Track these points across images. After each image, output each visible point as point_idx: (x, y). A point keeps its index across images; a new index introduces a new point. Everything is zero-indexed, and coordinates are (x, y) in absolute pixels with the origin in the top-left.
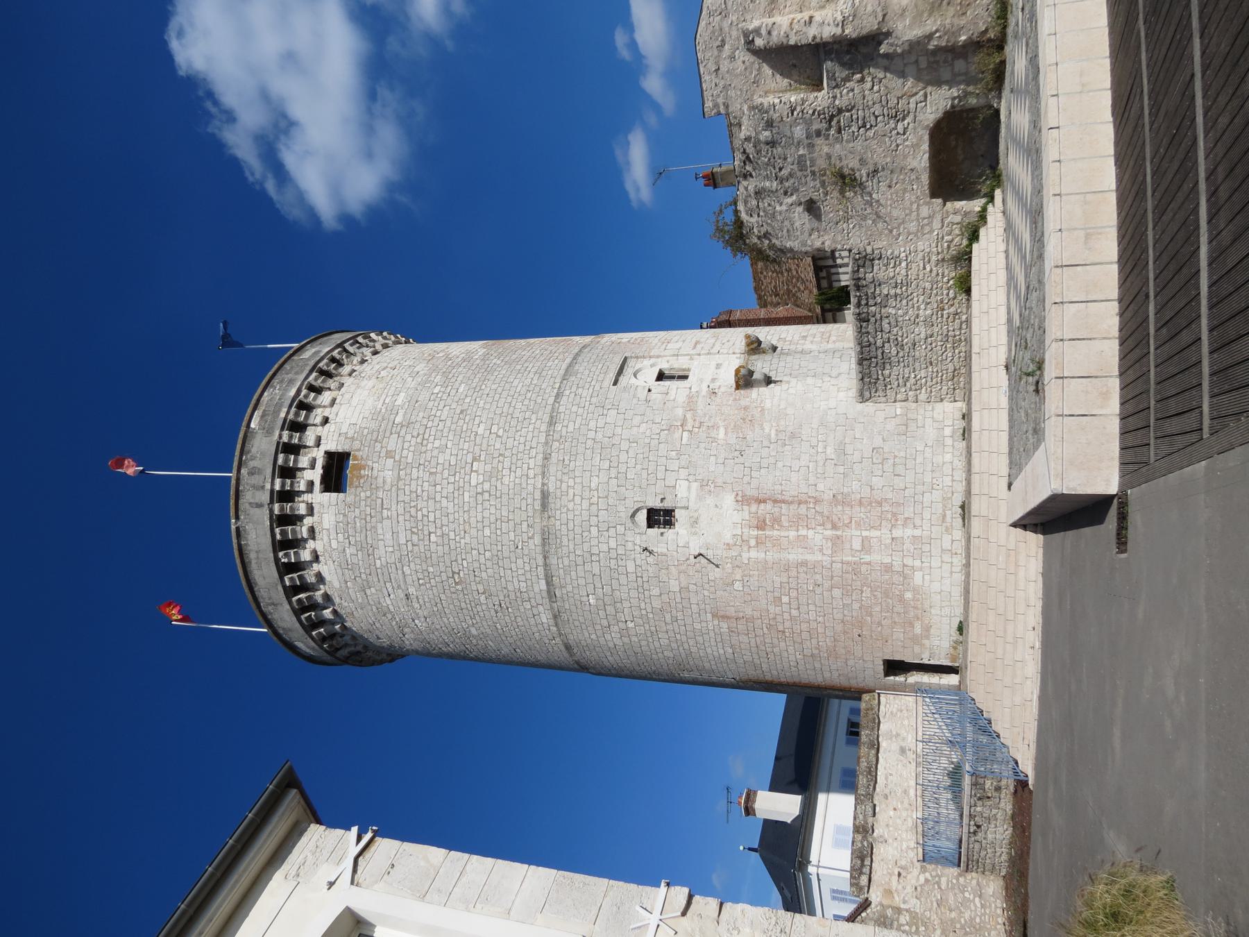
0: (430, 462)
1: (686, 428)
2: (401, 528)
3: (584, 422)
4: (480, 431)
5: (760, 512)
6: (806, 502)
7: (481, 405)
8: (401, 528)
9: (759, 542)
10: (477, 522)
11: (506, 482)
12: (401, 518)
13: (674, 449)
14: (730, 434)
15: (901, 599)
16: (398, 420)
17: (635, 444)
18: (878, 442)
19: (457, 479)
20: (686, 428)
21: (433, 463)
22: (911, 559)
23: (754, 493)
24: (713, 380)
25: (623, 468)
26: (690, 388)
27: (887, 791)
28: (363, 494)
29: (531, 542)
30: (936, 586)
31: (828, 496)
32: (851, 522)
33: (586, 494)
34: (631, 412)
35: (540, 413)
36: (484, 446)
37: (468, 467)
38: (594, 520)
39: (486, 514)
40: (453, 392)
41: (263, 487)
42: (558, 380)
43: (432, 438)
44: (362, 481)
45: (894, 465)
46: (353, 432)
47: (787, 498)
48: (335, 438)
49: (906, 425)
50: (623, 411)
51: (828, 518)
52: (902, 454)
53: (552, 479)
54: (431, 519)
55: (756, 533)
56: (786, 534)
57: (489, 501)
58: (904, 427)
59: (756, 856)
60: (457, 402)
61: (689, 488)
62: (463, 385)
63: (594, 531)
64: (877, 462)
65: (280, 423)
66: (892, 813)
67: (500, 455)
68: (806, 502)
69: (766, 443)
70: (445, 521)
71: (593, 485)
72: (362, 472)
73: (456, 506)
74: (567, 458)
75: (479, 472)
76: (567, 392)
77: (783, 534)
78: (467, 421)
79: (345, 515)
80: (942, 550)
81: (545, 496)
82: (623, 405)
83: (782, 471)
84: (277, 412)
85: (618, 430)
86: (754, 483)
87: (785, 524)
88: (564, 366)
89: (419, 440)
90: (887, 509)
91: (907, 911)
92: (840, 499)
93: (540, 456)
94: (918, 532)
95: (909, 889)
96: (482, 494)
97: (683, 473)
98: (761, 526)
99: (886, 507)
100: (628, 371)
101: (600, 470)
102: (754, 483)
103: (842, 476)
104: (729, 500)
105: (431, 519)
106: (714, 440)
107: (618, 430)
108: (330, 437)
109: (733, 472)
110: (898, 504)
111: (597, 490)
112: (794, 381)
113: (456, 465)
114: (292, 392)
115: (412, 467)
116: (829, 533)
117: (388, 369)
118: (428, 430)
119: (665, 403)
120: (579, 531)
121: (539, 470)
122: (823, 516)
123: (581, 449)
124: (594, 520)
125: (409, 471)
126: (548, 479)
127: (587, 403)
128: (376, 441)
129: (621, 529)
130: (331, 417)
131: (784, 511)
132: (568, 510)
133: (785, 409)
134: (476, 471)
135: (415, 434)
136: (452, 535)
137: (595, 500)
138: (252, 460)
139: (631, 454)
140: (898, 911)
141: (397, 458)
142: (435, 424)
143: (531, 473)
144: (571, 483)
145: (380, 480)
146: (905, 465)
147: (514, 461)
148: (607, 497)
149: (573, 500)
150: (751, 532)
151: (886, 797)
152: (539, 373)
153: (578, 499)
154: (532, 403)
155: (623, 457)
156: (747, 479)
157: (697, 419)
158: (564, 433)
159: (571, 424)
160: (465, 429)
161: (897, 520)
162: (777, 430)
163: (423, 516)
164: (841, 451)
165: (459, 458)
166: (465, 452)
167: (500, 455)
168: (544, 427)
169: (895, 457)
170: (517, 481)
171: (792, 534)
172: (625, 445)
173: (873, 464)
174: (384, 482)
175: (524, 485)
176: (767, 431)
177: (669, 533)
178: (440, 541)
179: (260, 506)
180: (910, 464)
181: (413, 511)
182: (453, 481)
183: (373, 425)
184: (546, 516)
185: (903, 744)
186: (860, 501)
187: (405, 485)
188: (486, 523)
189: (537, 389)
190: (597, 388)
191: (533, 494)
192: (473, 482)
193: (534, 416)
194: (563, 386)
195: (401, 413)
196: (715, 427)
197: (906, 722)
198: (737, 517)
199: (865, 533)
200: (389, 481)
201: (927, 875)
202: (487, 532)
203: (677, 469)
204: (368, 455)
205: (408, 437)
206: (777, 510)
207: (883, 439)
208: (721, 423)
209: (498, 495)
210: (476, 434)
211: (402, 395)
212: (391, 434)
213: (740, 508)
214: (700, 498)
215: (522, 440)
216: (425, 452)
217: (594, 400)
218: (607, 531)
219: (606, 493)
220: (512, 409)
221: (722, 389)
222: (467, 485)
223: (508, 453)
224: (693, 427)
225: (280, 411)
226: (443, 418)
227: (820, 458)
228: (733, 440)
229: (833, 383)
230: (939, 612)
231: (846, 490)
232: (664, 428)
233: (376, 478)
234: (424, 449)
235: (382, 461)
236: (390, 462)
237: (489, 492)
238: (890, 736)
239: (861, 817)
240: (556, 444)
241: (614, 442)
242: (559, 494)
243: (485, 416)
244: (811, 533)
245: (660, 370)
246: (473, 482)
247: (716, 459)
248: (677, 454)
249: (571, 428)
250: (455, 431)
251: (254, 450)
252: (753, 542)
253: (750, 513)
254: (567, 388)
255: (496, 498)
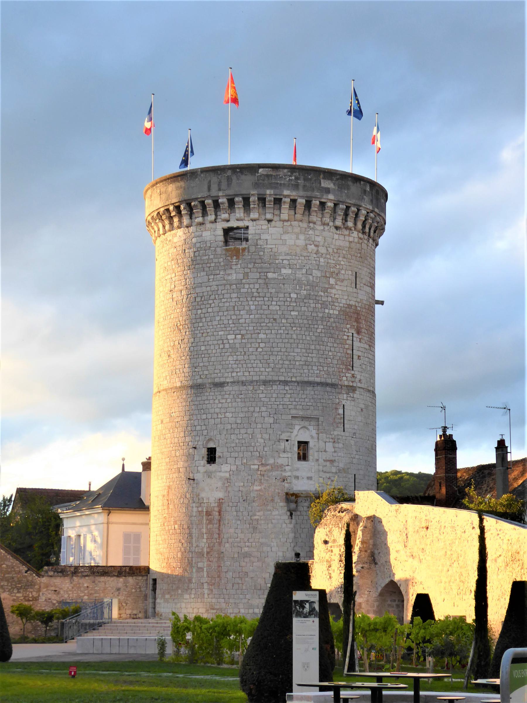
0: (241, 305)
1: (260, 467)
2: (204, 289)
3: (265, 403)
4: (262, 336)
5: (214, 512)
6: (219, 537)
7: (280, 332)
8: (204, 289)
9: (200, 512)
10: (208, 341)
11: (230, 358)
12: (208, 289)
13: (248, 461)
14: (256, 493)
15: (178, 588)
16: (270, 275)
17: (251, 437)
18: (251, 575)
19: (231, 325)
20: (260, 467)
21: (241, 308)
22: (194, 593)
23: (223, 509)
24: (297, 478)
25: (237, 431)
26: (288, 465)
27: (96, 582)
28: (222, 259)
29: (198, 377)
30: (183, 605)
31: (223, 549)
32: (210, 562)
33: (223, 410)
34: (271, 432)
35: (272, 373)
36: (250, 341)
37: (238, 332)
38: (209, 416)
39: (212, 347)
40: (290, 308)
41: (220, 190)
42: (298, 379)
43: (256, 303)
44: (229, 258)
45: (238, 583)
46: (262, 243)
47: (221, 527)
48: (257, 232)
49: (260, 589)
50: (272, 427)
51: (212, 549)
52: (244, 587)
53: (231, 389)
54: (210, 310)
55: (205, 510)
56: (204, 527)
57: (219, 348)
58: (259, 588)
59: (120, 471)
60: (282, 314)
61: (226, 472)
62: (296, 313)
63: (204, 417)
64: (240, 575)
65: (261, 192)
66: (86, 585)
67: (245, 353)
68: (219, 537)
69: (251, 514)
70: (208, 319)
71: (227, 414)
72: (235, 257)
73: (216, 327)
74: (242, 396)
75: (235, 340)
76: (287, 388)
77: (204, 525)
78: (268, 325)
79: (210, 247)
80: (198, 609)
81: (221, 385)
82: (276, 426)
83: (235, 523)
84: (271, 186)
85: (259, 426)
86: (229, 509)
87: (209, 527)
88: (311, 379)
89: (255, 294)
90: (217, 580)
91: (39, 595)
92: (221, 556)
93: (244, 379)
94: (206, 596)
95: (49, 596)
96: (223, 343)
97: (234, 468)
98: (208, 514)
99: (217, 580)
100: (306, 423)
101: (236, 417)
102: (229, 509)
103: (233, 556)
104: (220, 495)
105: (210, 310)
106: (253, 484)
107: (259, 426)
108: (258, 227)
109: (235, 496)
110: (219, 586)
111: (225, 417)
112: (291, 526)
113: (240, 323)
114: (286, 192)
115: (238, 293)
116: (205, 550)
117: (315, 249)
118: (262, 299)
119: (277, 451)
120: (204, 406)
121: (236, 379)
122: (213, 546)
123: (248, 404)
124: (209, 416)
125: (235, 291)
126: (231, 386)
127: (279, 403)
128: (255, 263)
129: (205, 432)
130: (273, 223)
131: (215, 525)
132: (215, 400)
133: (272, 523)
134: (235, 338)
135: (259, 290)
136: (201, 325)
137: (220, 416)
138: (237, 177)
139: (245, 436)
140: (39, 590)
141: (244, 281)
142: (266, 303)
143: (234, 374)
144: (229, 400)
145: (228, 272)
146: (238, 589)
147: (241, 362)
148: (221, 423)
149: (220, 403)
150: (205, 508)
151: (94, 582)
152: (307, 364)
153: (220, 405)
154: (280, 366)
155: (243, 431)
156: (231, 504)
157: (266, 473)
158: (258, 392)
159: (264, 395)
160: (262, 325)
161: (211, 585)
162: (258, 519)
163: (211, 304)
164: (247, 555)
165: (244, 325)
166: (247, 328)
167: (245, 353)
168: (263, 378)
169: (243, 584)
170: (230, 366)
171: (204, 531)
172: (250, 431)
173: (239, 572)
174: (229, 274)
175: (228, 371)
176: (258, 514)
177: (204, 462)
178: (198, 316)
179: (209, 189)
180: (239, 592)
181: (213, 297)
182: (230, 323)
183: (266, 258)
184: (211, 386)
185: (122, 590)
186: (220, 566)
187: (227, 290)
188: (208, 347)
189: (292, 366)
190: (290, 407)
191: (222, 377)
192: (229, 337)
193: (270, 369)
194: (292, 384)
195: (275, 276)
196: (261, 483)
197: (133, 590)
198: (212, 500)
199: (205, 569)
200: (230, 278)
201: (57, 604)
202: (203, 348)
203: (236, 464)
204: (245, 259)
205: (257, 286)
206: (216, 522)
207: (253, 577)
208: (263, 487)
209: (223, 354)
210: (258, 333)
211: (290, 271)
212: (260, 273)
213: (216, 501)
214: (221, 478)
215: (255, 365)
216: (247, 300)
217: (281, 407)
218: (204, 425)
219: (223, 423)
220: (276, 353)
221: (287, 485)
222: (227, 333)
223: (246, 357)
224: (261, 471)
225: (271, 188)
226: (271, 308)
227: (242, 544)
228: (252, 495)
229: (289, 548)
230: (173, 607)
231: (225, 558)
232: (261, 454)
233: (231, 268)
234: (249, 299)
235: (242, 271)
236: (241, 276)
237: (224, 348)
238: (125, 583)
239: (83, 570)
240: (252, 388)
241: (252, 424)
242: (223, 393)
243: (272, 336)
244: (205, 540)
245: (309, 442)
246: (229, 337)
247: (242, 486)
248: (245, 463)
249: (261, 396)
250: (261, 318)
251: (243, 177)
252: (200, 509)
253: (214, 507)
254: (291, 387)
255: (221, 353)
